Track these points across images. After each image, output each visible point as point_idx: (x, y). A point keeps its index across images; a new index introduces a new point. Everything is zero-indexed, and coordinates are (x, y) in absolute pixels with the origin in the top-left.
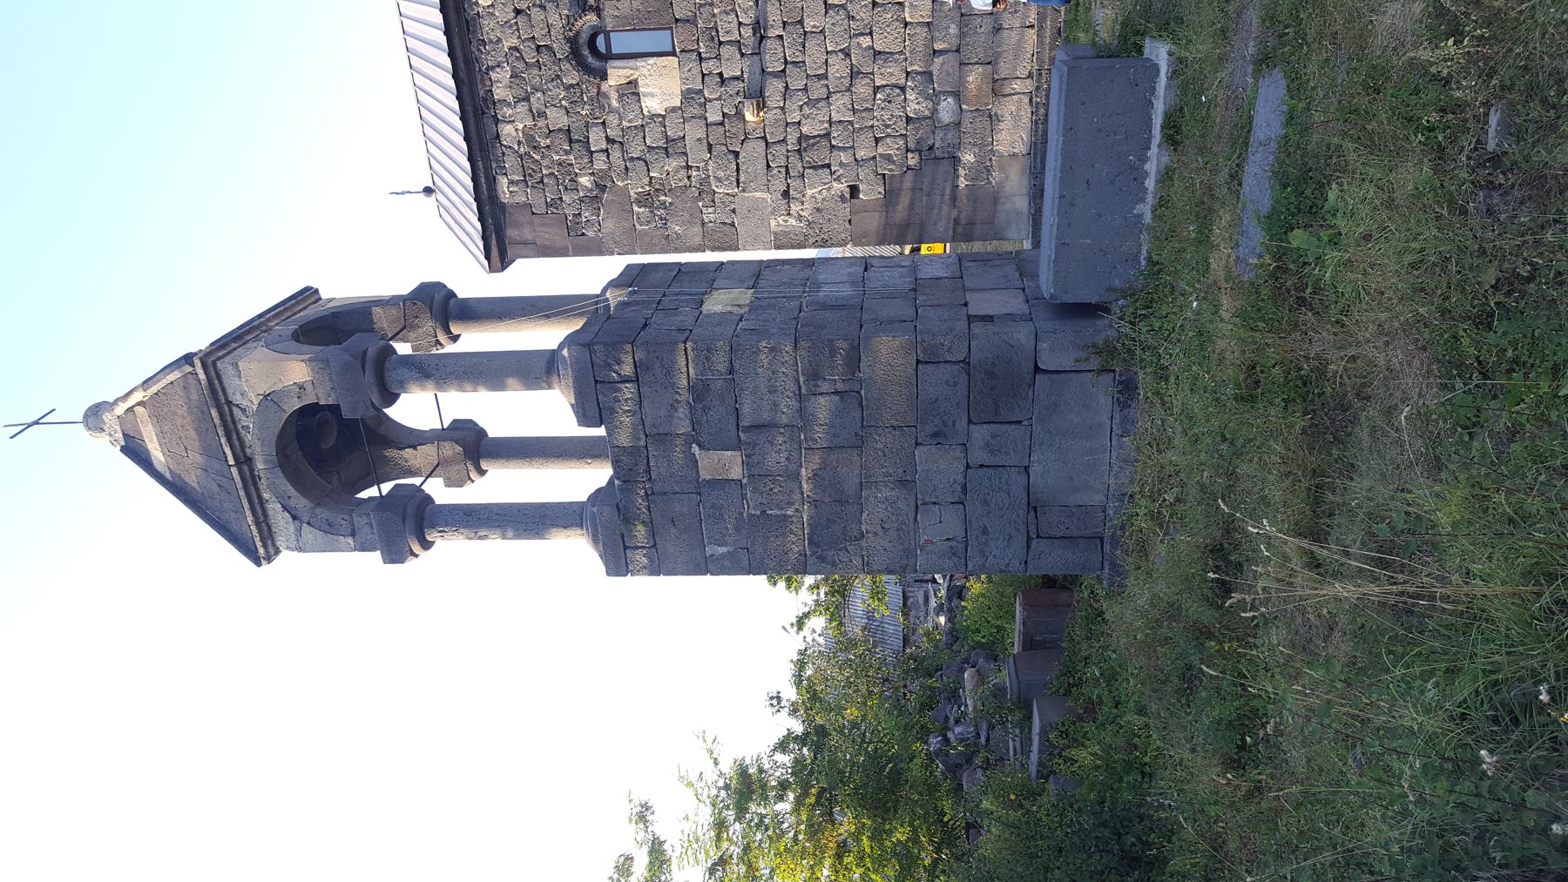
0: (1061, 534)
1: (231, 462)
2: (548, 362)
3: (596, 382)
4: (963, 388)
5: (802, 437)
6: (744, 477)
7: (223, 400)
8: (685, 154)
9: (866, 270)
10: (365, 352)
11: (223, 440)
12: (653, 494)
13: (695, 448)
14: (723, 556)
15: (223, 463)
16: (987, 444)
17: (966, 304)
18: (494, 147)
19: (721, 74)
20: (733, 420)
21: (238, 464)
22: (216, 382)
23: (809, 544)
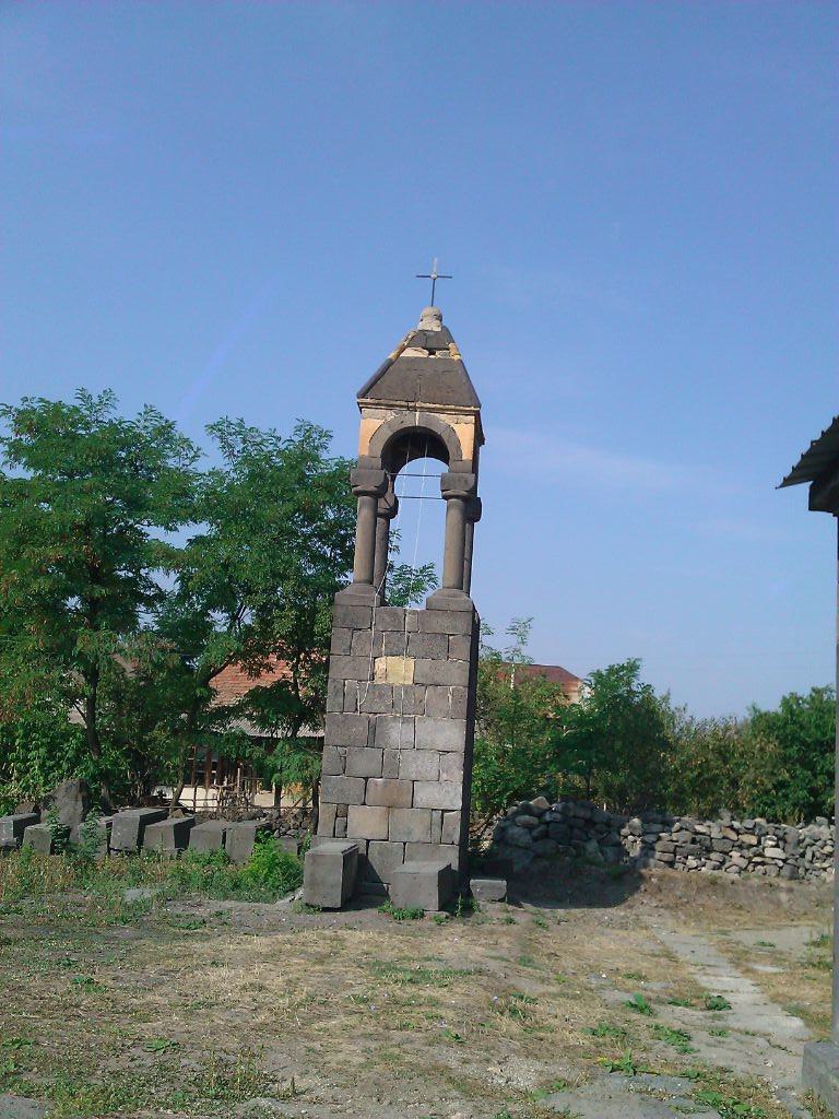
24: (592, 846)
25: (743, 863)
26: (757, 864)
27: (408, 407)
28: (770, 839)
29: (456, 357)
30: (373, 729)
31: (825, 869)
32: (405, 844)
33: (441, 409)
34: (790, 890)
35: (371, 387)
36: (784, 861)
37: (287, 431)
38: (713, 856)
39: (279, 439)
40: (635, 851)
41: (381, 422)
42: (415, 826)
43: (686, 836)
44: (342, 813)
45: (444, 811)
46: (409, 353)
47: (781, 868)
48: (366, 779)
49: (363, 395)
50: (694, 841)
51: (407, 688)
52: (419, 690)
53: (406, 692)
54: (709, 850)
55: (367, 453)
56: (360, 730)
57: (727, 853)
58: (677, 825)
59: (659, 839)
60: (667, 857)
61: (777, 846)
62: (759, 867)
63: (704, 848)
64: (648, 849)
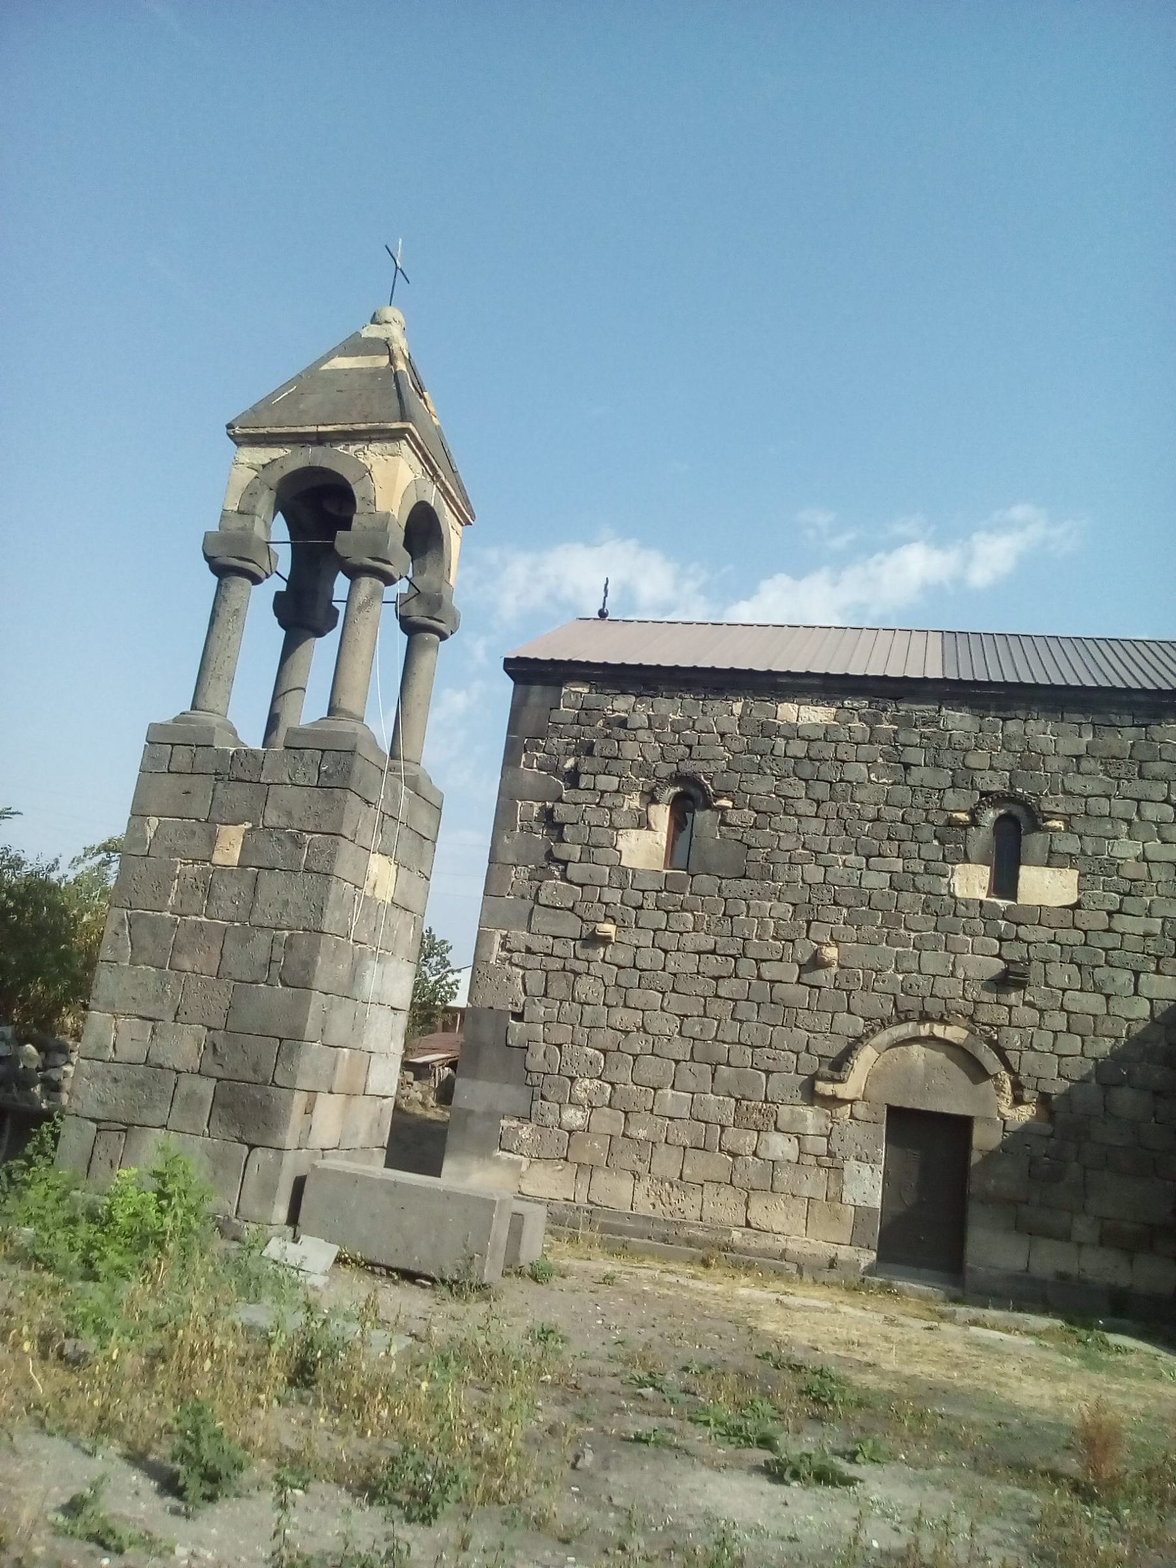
0: (96, 1152)
1: (321, 429)
2: (351, 713)
3: (323, 751)
4: (250, 1076)
5: (236, 924)
6: (213, 865)
7: (374, 436)
8: (580, 861)
9: (393, 1008)
10: (388, 563)
11: (339, 427)
12: (216, 780)
13: (249, 825)
14: (144, 832)
15: (321, 422)
16: (194, 1093)
17: (331, 1092)
18: (616, 688)
19: (641, 907)
20: (267, 864)
21: (318, 433)
22: (388, 435)
23: (139, 914)
33: (452, 499)
56: (343, 968)
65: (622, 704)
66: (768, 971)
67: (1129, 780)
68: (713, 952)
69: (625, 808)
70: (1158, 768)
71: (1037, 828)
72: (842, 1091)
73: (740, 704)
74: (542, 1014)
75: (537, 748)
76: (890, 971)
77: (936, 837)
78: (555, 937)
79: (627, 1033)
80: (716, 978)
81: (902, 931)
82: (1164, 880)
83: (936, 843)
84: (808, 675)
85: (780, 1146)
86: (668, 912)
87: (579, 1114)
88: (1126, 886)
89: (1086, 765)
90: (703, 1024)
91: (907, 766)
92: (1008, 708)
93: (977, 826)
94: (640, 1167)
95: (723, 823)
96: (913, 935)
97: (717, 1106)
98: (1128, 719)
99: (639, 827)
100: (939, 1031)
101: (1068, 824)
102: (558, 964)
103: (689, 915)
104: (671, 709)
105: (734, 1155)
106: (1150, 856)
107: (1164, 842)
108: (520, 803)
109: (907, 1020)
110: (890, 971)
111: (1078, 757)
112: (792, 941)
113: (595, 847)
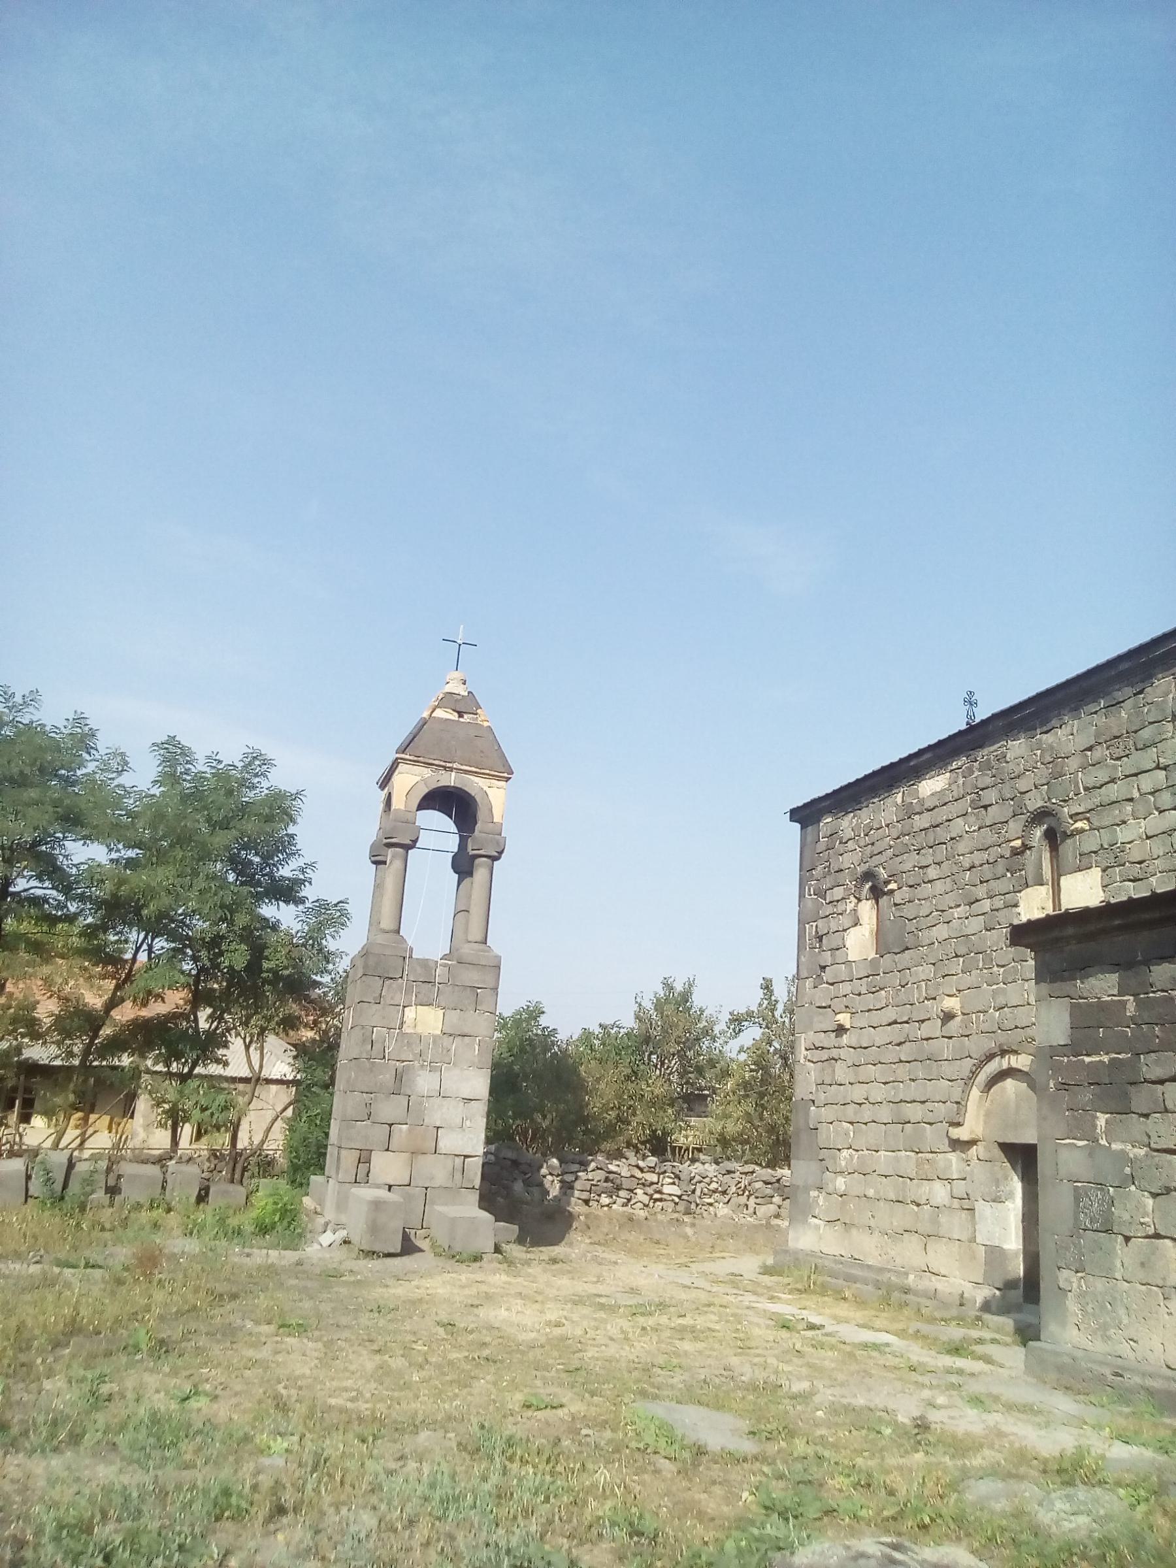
19: (859, 994)
24: (518, 1187)
25: (646, 1199)
26: (656, 1200)
27: (445, 768)
28: (669, 1177)
29: (486, 724)
30: (399, 1077)
31: (711, 1204)
32: (426, 1188)
33: (476, 772)
34: (693, 1225)
35: (411, 742)
36: (679, 1197)
37: (232, 755)
38: (622, 1193)
39: (220, 762)
40: (554, 1190)
41: (418, 778)
42: (437, 1172)
43: (601, 1175)
44: (364, 1158)
45: (466, 1157)
46: (440, 713)
47: (676, 1204)
48: (391, 1125)
49: (403, 749)
50: (607, 1180)
51: (435, 1037)
52: (447, 1041)
53: (434, 1042)
54: (619, 1188)
55: (402, 808)
56: (387, 1077)
57: (631, 1191)
58: (593, 1165)
59: (577, 1178)
60: (585, 1195)
61: (674, 1183)
62: (658, 1203)
63: (614, 1186)
64: (567, 1187)
65: (847, 824)
66: (926, 1030)
67: (1127, 756)
68: (895, 1022)
69: (848, 911)
70: (1146, 734)
71: (1067, 836)
72: (962, 1134)
73: (901, 794)
74: (823, 1098)
75: (812, 878)
76: (992, 1010)
77: (1008, 870)
78: (825, 1032)
79: (860, 1104)
80: (899, 1044)
81: (995, 969)
82: (1161, 854)
83: (1009, 875)
84: (921, 752)
85: (939, 1193)
86: (873, 993)
87: (844, 1180)
88: (1136, 871)
89: (1098, 753)
90: (894, 1088)
91: (985, 807)
92: (1048, 721)
93: (1030, 848)
94: (872, 1223)
95: (896, 905)
96: (1002, 969)
97: (908, 1161)
98: (1129, 691)
99: (856, 925)
100: (1016, 1062)
101: (1088, 819)
102: (825, 1055)
103: (883, 992)
104: (865, 816)
105: (918, 1205)
106: (1149, 834)
107: (1160, 812)
108: (807, 926)
109: (990, 1057)
110: (992, 1010)
111: (1090, 749)
112: (935, 999)
113: (837, 949)
